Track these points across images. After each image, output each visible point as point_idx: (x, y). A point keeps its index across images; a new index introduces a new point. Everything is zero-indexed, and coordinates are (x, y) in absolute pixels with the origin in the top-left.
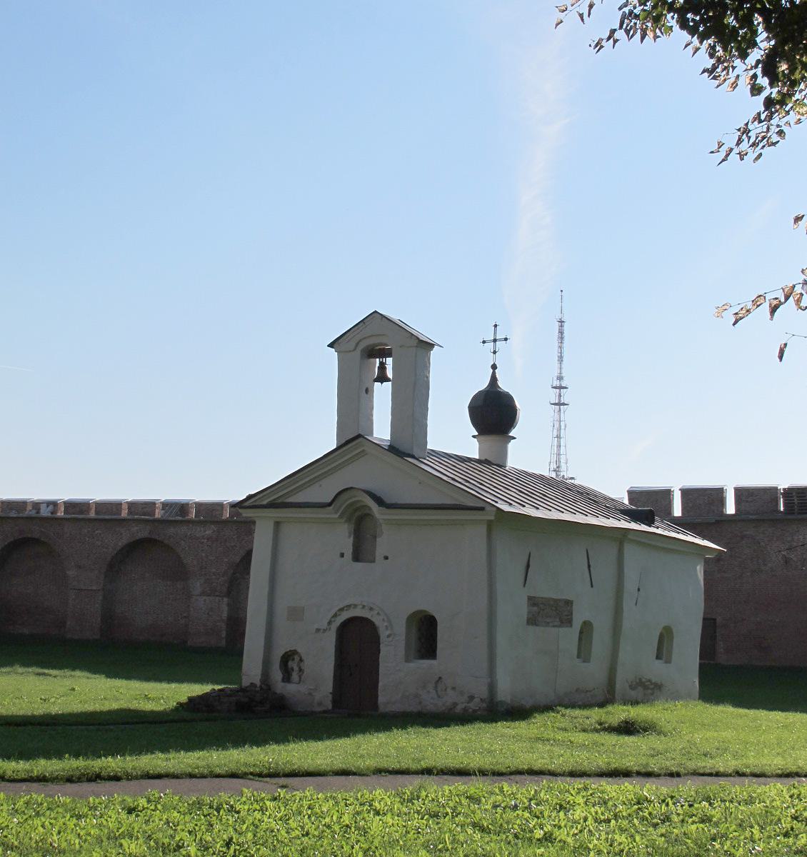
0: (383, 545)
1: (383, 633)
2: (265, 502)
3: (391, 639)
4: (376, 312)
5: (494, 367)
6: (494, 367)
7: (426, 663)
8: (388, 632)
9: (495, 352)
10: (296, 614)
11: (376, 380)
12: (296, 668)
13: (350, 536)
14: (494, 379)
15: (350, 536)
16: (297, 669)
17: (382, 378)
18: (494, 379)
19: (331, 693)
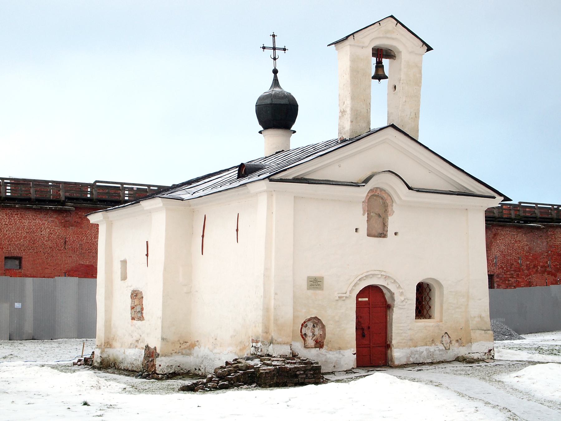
0: (394, 223)
1: (398, 299)
2: (291, 177)
3: (404, 303)
4: (392, 17)
5: (275, 72)
6: (275, 72)
7: (423, 322)
8: (402, 298)
9: (275, 59)
10: (315, 283)
11: (374, 78)
12: (309, 334)
13: (364, 214)
14: (276, 82)
15: (364, 214)
16: (312, 334)
17: (379, 76)
18: (276, 82)
19: (354, 354)
